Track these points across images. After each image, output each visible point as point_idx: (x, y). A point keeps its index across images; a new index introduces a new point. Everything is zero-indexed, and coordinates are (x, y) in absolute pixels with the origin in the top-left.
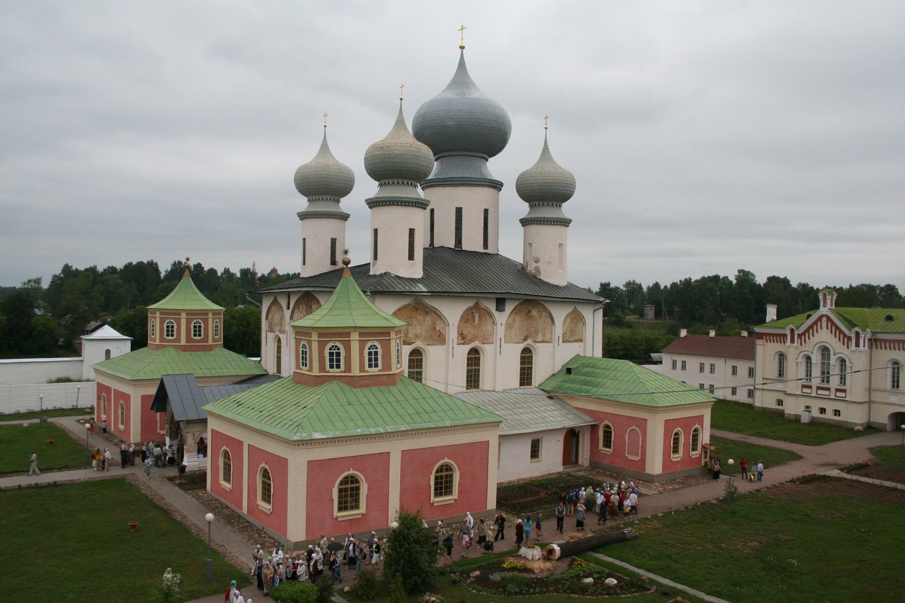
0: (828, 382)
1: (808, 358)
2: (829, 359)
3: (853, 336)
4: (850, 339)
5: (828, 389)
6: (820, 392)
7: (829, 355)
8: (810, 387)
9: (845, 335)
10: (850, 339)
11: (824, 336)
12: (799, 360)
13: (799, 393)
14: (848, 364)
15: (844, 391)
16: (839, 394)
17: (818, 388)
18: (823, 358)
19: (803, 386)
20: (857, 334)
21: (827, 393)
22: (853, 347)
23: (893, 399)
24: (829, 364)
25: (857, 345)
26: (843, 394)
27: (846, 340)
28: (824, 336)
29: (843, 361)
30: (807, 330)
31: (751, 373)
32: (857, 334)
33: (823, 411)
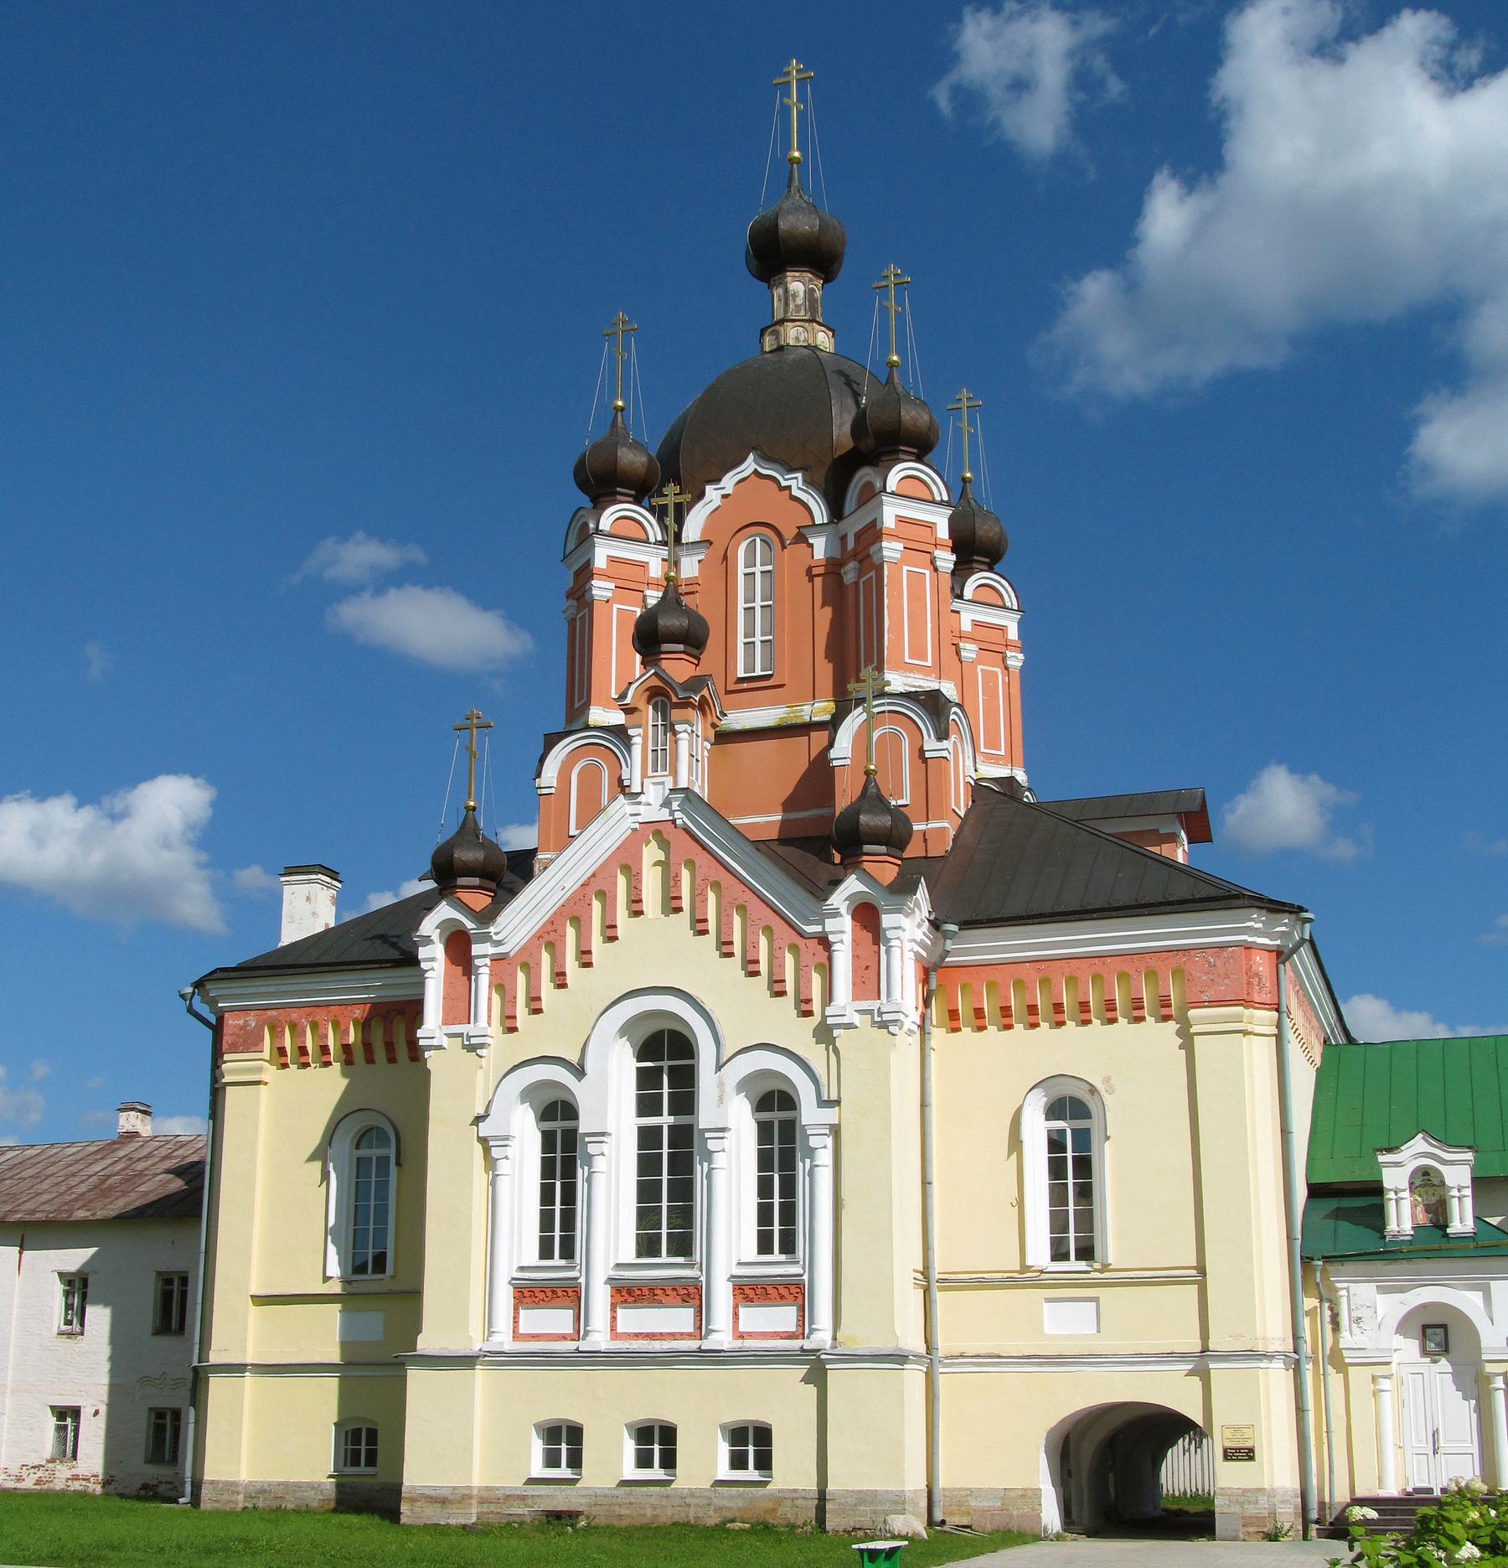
0: (682, 1246)
1: (559, 1117)
11: (662, 954)
14: (809, 1113)
15: (794, 1292)
16: (757, 1318)
19: (529, 1294)
20: (867, 916)
21: (680, 1318)
30: (548, 936)
33: (657, 1441)
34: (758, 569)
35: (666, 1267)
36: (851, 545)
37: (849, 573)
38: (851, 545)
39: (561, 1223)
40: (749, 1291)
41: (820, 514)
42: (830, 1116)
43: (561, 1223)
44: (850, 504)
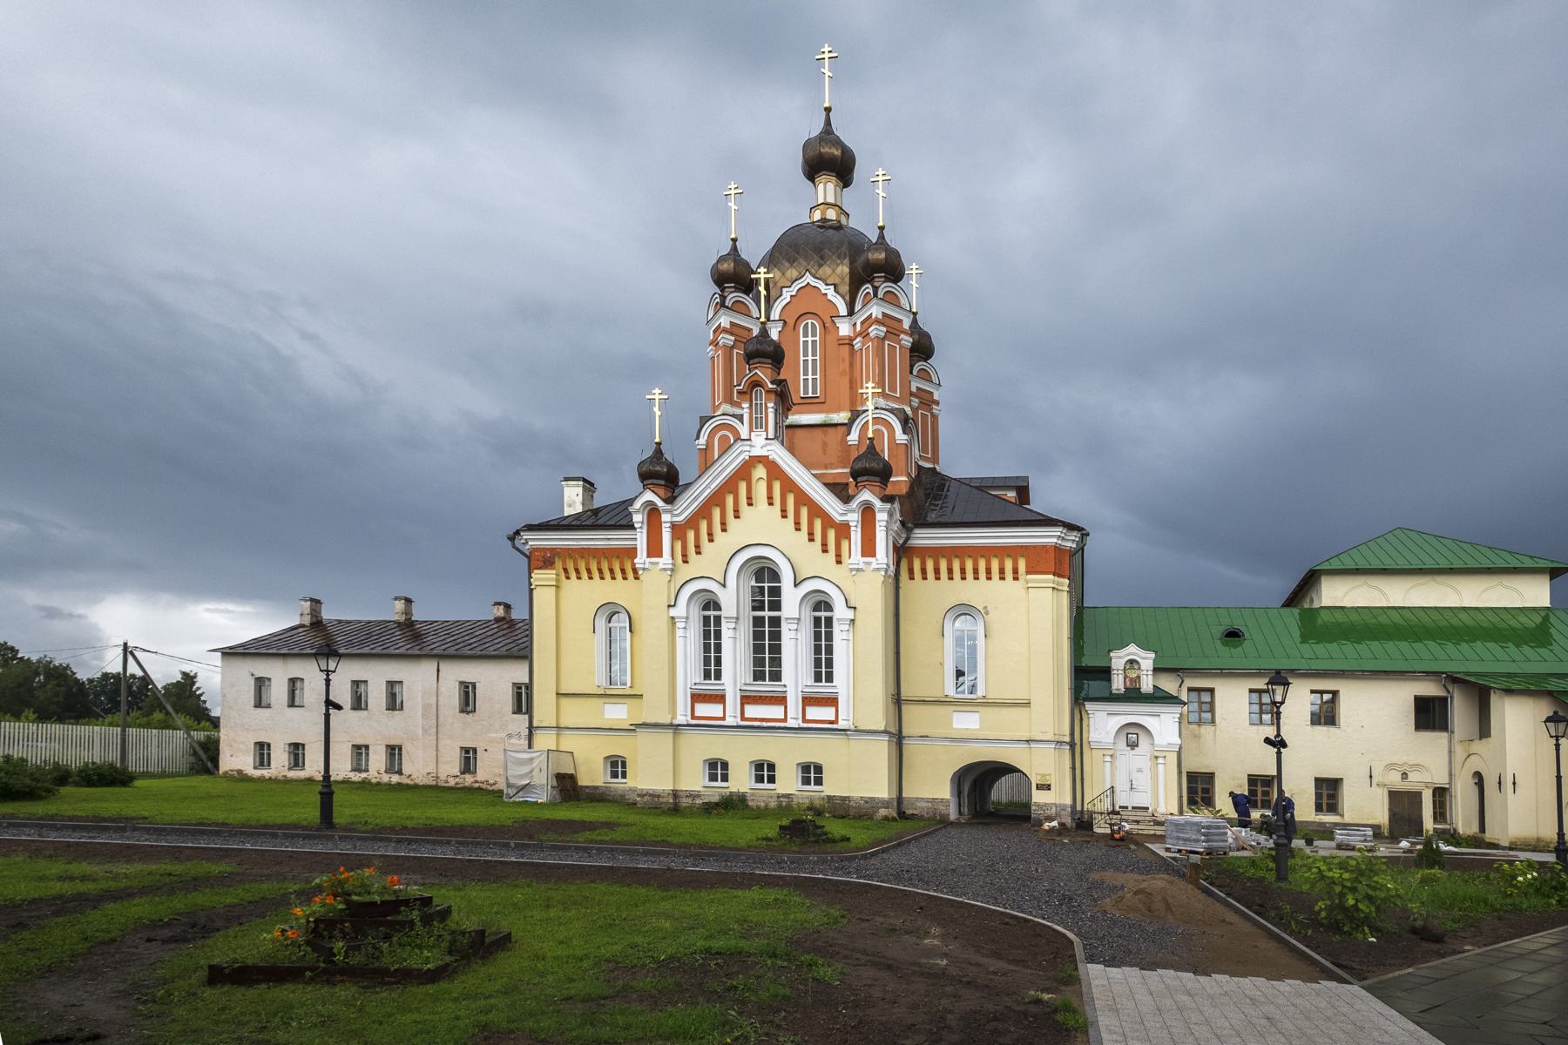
0: (776, 676)
2: (776, 606)
3: (854, 518)
4: (843, 530)
5: (781, 700)
6: (753, 711)
7: (776, 592)
8: (720, 698)
9: (828, 521)
10: (843, 530)
12: (680, 611)
13: (682, 718)
14: (840, 612)
15: (832, 701)
16: (814, 713)
17: (747, 699)
18: (758, 606)
19: (698, 698)
20: (868, 511)
21: (775, 712)
22: (855, 557)
23: (966, 722)
24: (776, 622)
25: (869, 549)
26: (826, 713)
27: (831, 534)
28: (761, 527)
29: (822, 604)
31: (523, 699)
32: (868, 511)
34: (810, 339)
35: (766, 687)
36: (858, 328)
37: (858, 343)
38: (858, 328)
39: (712, 665)
40: (809, 701)
41: (843, 310)
42: (850, 614)
43: (712, 665)
44: (858, 307)
